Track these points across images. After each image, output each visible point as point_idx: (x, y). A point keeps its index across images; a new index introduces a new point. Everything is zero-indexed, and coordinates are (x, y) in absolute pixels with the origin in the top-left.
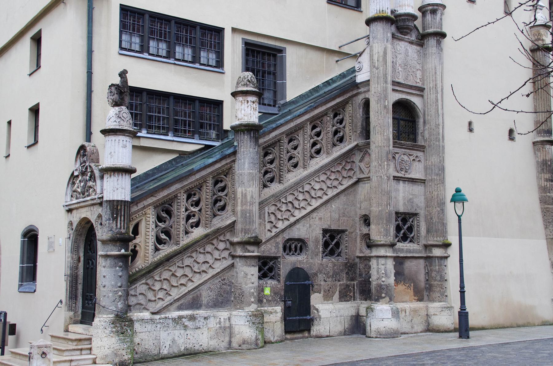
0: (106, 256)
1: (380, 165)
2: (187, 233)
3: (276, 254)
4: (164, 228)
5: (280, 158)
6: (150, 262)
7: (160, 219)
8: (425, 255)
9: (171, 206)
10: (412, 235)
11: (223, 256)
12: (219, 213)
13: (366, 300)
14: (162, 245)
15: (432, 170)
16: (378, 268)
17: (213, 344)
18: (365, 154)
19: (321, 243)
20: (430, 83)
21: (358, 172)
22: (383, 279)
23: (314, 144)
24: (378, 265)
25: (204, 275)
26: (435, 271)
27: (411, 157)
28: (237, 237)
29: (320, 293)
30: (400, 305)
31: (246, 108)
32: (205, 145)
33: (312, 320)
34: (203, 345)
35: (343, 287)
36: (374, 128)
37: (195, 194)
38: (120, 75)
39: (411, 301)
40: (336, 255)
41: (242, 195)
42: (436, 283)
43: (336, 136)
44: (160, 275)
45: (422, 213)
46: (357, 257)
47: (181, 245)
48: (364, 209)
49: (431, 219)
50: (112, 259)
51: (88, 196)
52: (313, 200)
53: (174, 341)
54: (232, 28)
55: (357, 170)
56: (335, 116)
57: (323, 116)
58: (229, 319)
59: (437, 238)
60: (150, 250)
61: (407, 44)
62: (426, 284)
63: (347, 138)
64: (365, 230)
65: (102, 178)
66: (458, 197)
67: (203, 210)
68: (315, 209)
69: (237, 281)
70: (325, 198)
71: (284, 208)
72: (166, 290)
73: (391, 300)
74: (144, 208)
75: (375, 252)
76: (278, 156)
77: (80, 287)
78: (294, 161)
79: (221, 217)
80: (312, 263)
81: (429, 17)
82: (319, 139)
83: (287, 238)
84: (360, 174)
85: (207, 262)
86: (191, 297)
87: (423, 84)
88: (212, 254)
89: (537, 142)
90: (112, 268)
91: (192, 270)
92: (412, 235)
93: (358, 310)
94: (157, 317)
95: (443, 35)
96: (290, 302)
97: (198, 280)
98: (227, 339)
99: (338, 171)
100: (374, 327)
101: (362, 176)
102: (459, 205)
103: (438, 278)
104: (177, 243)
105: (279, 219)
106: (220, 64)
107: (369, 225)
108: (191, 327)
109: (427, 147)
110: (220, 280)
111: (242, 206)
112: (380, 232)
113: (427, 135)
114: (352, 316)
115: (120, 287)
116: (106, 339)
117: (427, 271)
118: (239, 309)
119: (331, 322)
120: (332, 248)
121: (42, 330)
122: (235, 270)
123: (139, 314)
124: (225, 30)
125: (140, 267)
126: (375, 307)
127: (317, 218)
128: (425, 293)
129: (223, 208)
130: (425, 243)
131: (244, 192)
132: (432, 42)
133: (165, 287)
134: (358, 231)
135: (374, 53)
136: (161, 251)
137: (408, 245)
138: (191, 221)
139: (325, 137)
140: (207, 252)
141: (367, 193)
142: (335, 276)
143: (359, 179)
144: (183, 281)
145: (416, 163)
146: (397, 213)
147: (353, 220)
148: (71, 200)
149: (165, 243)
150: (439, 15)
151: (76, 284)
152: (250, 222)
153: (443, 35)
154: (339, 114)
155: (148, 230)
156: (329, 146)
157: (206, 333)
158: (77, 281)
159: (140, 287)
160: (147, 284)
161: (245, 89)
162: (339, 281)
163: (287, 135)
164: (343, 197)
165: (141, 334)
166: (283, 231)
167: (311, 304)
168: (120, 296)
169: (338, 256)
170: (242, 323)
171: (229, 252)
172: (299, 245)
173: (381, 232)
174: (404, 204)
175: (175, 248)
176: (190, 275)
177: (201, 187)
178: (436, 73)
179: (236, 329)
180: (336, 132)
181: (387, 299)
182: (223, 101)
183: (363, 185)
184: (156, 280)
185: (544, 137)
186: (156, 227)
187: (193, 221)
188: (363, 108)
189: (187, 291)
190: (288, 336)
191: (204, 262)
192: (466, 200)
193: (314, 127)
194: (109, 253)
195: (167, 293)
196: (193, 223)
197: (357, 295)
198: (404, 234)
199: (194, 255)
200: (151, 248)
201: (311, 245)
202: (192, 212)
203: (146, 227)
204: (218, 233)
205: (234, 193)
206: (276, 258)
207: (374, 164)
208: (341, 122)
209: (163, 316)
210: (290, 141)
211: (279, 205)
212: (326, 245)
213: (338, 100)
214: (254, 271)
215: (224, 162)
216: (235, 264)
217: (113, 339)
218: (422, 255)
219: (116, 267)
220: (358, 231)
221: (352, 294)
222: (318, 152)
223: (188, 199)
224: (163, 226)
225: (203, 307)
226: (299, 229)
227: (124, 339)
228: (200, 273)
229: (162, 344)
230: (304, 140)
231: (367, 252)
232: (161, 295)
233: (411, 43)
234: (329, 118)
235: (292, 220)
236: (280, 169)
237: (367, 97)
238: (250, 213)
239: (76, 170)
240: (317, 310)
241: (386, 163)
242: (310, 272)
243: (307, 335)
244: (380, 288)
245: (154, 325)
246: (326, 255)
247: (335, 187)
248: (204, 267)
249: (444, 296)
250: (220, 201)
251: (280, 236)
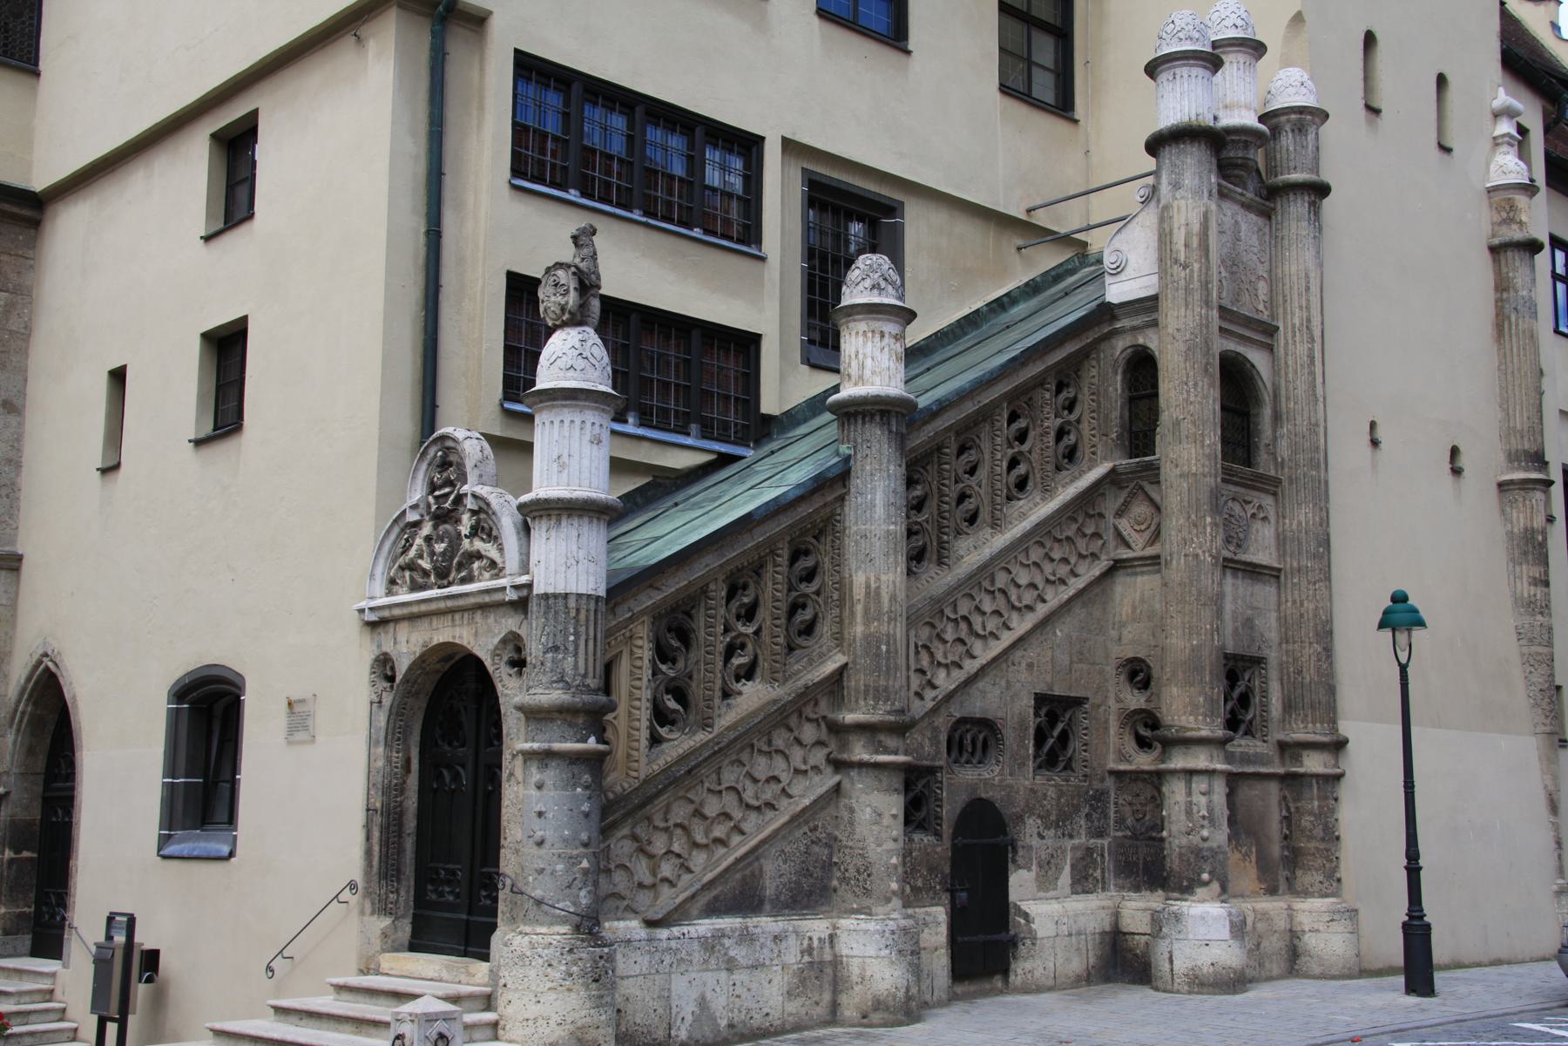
0: (545, 757)
1: (1195, 526)
2: (726, 694)
3: (933, 759)
4: (673, 679)
5: (942, 494)
6: (642, 777)
7: (663, 654)
8: (1281, 771)
9: (690, 617)
10: (1249, 717)
11: (812, 762)
12: (800, 641)
13: (1137, 889)
14: (666, 729)
15: (1300, 543)
17: (793, 1007)
18: (1132, 495)
19: (1032, 731)
20: (1292, 313)
21: (1112, 543)
22: (1205, 833)
23: (1014, 463)
24: (1189, 794)
25: (770, 814)
26: (1311, 813)
27: (1247, 507)
28: (851, 711)
29: (1029, 870)
30: (1247, 906)
31: (877, 353)
32: (720, 454)
33: (1014, 943)
34: (772, 1012)
35: (1079, 854)
36: (1177, 423)
37: (745, 587)
38: (575, 238)
39: (1255, 894)
40: (1062, 765)
41: (868, 594)
42: (1312, 845)
43: (1062, 444)
44: (666, 813)
45: (1273, 656)
46: (1112, 773)
47: (716, 730)
49: (1300, 672)
51: (469, 579)
52: (1015, 615)
53: (703, 1003)
54: (784, 139)
55: (1109, 536)
56: (1058, 391)
57: (1034, 388)
58: (831, 937)
59: (1314, 723)
60: (644, 743)
61: (1236, 208)
62: (1283, 848)
63: (1085, 451)
64: (1135, 700)
65: (526, 530)
66: (1400, 616)
67: (765, 632)
68: (1021, 639)
69: (853, 833)
70: (1042, 610)
71: (949, 635)
72: (679, 856)
73: (1224, 889)
74: (631, 619)
75: (1178, 761)
76: (935, 490)
77: (409, 844)
78: (970, 505)
79: (806, 651)
80: (1011, 786)
81: (1287, 140)
82: (1025, 447)
83: (958, 715)
84: (1116, 548)
85: (776, 779)
86: (738, 876)
87: (1272, 316)
88: (787, 758)
89: (1512, 482)
90: (564, 788)
91: (741, 799)
92: (1249, 717)
93: (1117, 915)
94: (663, 933)
95: (1322, 190)
96: (964, 895)
97: (758, 828)
98: (827, 996)
99: (1068, 538)
100: (1180, 965)
101: (1125, 554)
102: (1402, 637)
103: (1319, 832)
104: (706, 724)
105: (939, 664)
106: (749, 234)
107: (1145, 685)
108: (743, 962)
109: (1285, 484)
110: (806, 829)
111: (867, 623)
112: (1196, 706)
113: (1284, 449)
114: (1103, 933)
115: (586, 845)
116: (552, 996)
117: (1284, 813)
118: (858, 912)
119: (1058, 951)
120: (1052, 748)
121: (269, 968)
122: (844, 801)
123: (616, 923)
124: (767, 142)
125: (618, 789)
126: (1185, 910)
127: (1024, 665)
128: (1283, 874)
129: (809, 629)
130: (1281, 736)
131: (873, 586)
132: (1297, 207)
133: (676, 848)
134: (1111, 702)
135: (1176, 225)
136: (665, 746)
137: (1243, 742)
138: (737, 661)
139: (1039, 445)
140: (777, 751)
141: (1142, 601)
142: (1061, 822)
143: (1116, 561)
144: (719, 831)
145: (1258, 525)
146: (1226, 656)
147: (1101, 672)
148: (389, 593)
149: (673, 723)
150: (1311, 137)
151: (400, 836)
152: (888, 668)
153: (1322, 190)
154: (1068, 386)
155: (637, 683)
156: (1050, 467)
157: (777, 979)
158: (401, 825)
159: (622, 847)
160: (635, 838)
161: (875, 299)
162: (1071, 837)
163: (958, 434)
164: (1079, 612)
165: (626, 982)
166: (950, 696)
167: (1013, 896)
168: (586, 872)
169: (1065, 768)
170: (872, 953)
171: (826, 751)
172: (981, 737)
173: (1187, 706)
174: (1236, 631)
175: (702, 737)
176: (737, 814)
177: (761, 566)
178: (1308, 289)
179: (855, 970)
180: (1061, 433)
181: (1216, 886)
182: (759, 336)
183: (1128, 579)
184: (656, 828)
185: (1526, 470)
186: (654, 674)
187: (742, 660)
188: (1124, 372)
189: (731, 859)
190: (959, 989)
191: (768, 781)
192: (1421, 623)
193: (1013, 417)
194: (557, 746)
195: (682, 865)
196: (740, 666)
197: (1110, 876)
198: (1232, 712)
199: (745, 757)
200: (644, 735)
201: (1009, 735)
202: (741, 634)
203: (632, 673)
204: (808, 695)
205: (843, 587)
206: (932, 771)
207: (1174, 524)
208: (1070, 406)
209: (676, 931)
210: (962, 450)
211: (940, 626)
212: (1040, 737)
213: (1070, 348)
214: (893, 804)
215: (818, 502)
216: (846, 785)
217: (573, 996)
218: (1272, 770)
219: (575, 786)
220: (1111, 702)
221: (1098, 874)
222: (1022, 484)
223: (730, 596)
224: (672, 674)
225: (767, 907)
226: (983, 692)
227: (602, 997)
228: (758, 809)
229: (674, 1011)
230: (993, 450)
231: (1144, 761)
232: (667, 869)
233: (1247, 206)
234: (1047, 395)
235: (971, 666)
236: (940, 527)
237: (1141, 341)
238: (888, 644)
239: (414, 507)
240: (1026, 916)
241: (1209, 520)
242: (1008, 812)
243: (999, 984)
244: (1197, 854)
245: (657, 956)
246: (1040, 767)
247: (1063, 582)
248: (769, 793)
249: (1332, 882)
250: (804, 607)
251: (943, 710)
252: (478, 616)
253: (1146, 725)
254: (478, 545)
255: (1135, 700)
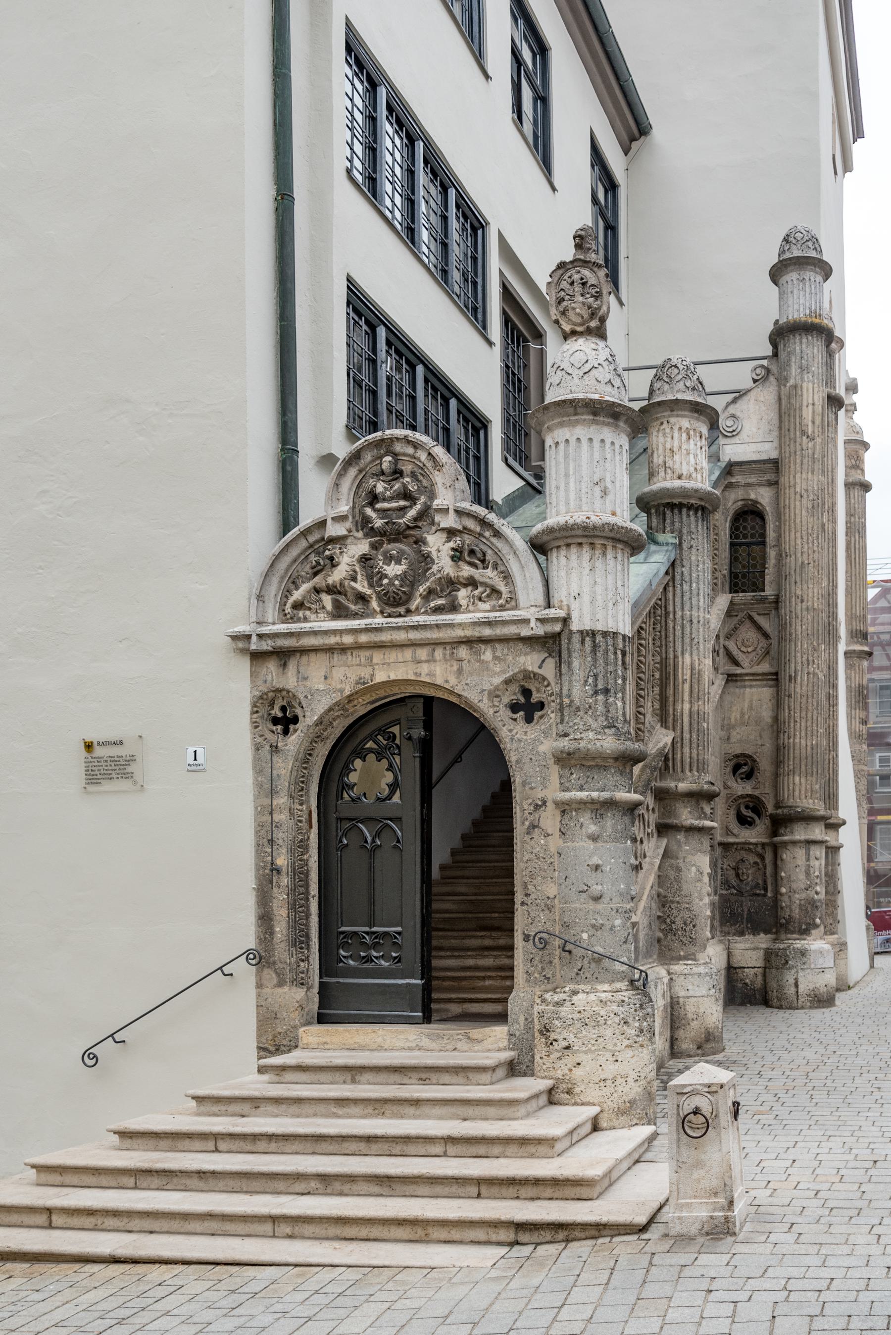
16: (809, 866)
24: (808, 860)
48: (740, 741)
50: (618, 815)
51: (454, 608)
64: (743, 788)
75: (800, 833)
90: (617, 840)
100: (802, 988)
126: (807, 946)
151: (307, 900)
252: (463, 652)
253: (747, 807)
254: (467, 571)
255: (743, 788)
